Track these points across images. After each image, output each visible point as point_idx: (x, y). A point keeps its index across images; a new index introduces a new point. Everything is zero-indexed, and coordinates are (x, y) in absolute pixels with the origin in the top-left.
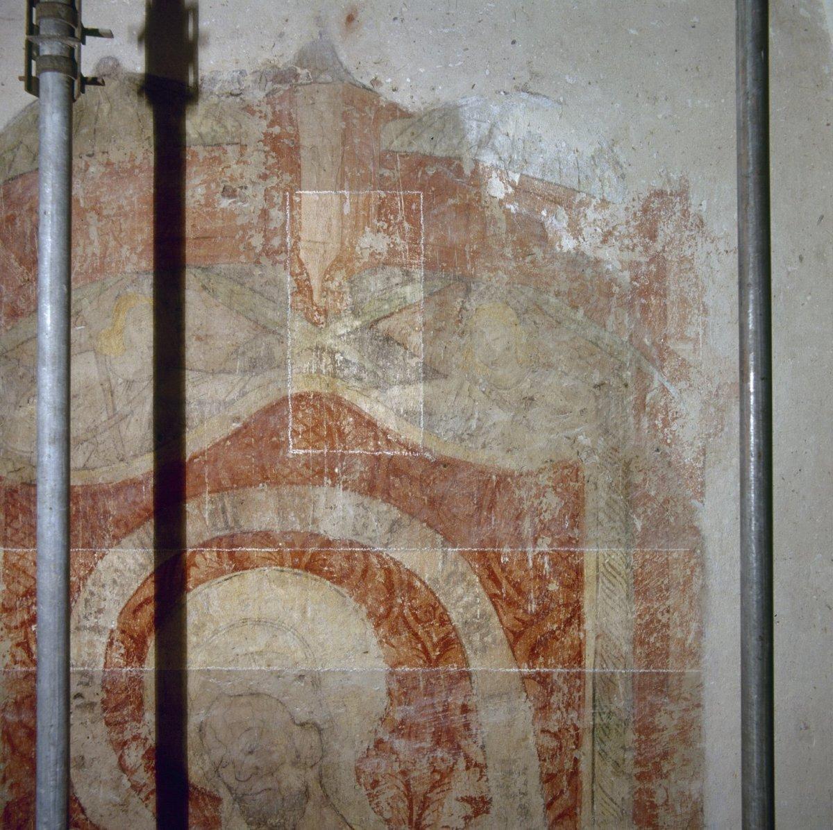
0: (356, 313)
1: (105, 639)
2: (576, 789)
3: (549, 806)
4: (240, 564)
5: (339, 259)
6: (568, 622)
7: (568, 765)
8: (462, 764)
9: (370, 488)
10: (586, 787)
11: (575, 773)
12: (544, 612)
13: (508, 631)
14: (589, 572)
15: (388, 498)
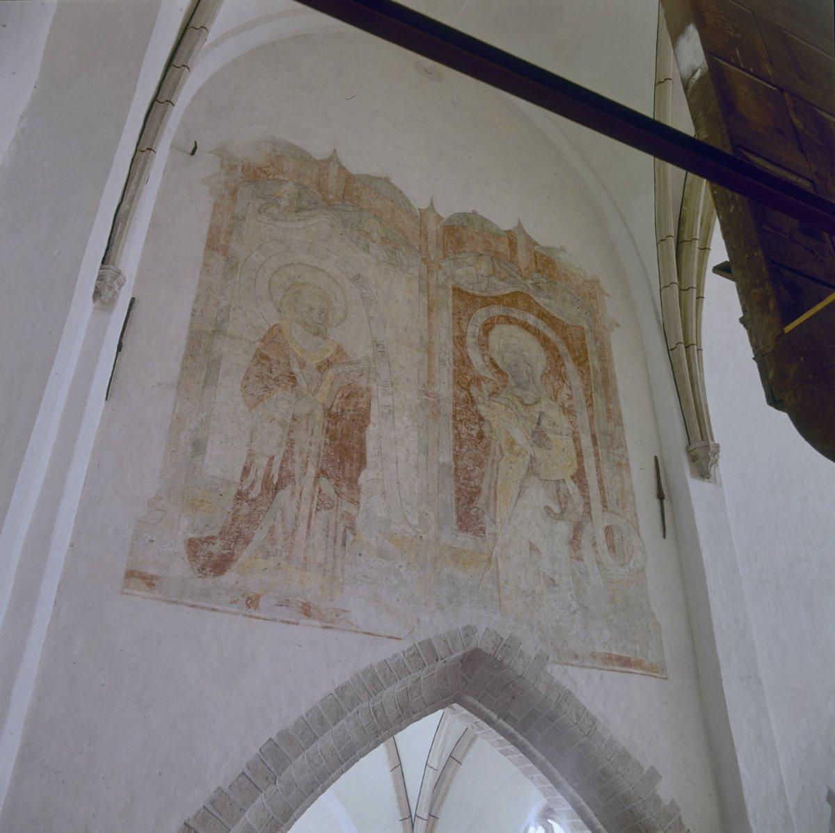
0: (532, 279)
1: (478, 329)
2: (592, 400)
3: (586, 402)
4: (510, 323)
5: (527, 268)
6: (585, 361)
7: (590, 393)
8: (565, 385)
9: (538, 316)
10: (594, 399)
11: (591, 396)
12: (580, 356)
13: (573, 358)
14: (589, 351)
15: (543, 320)
